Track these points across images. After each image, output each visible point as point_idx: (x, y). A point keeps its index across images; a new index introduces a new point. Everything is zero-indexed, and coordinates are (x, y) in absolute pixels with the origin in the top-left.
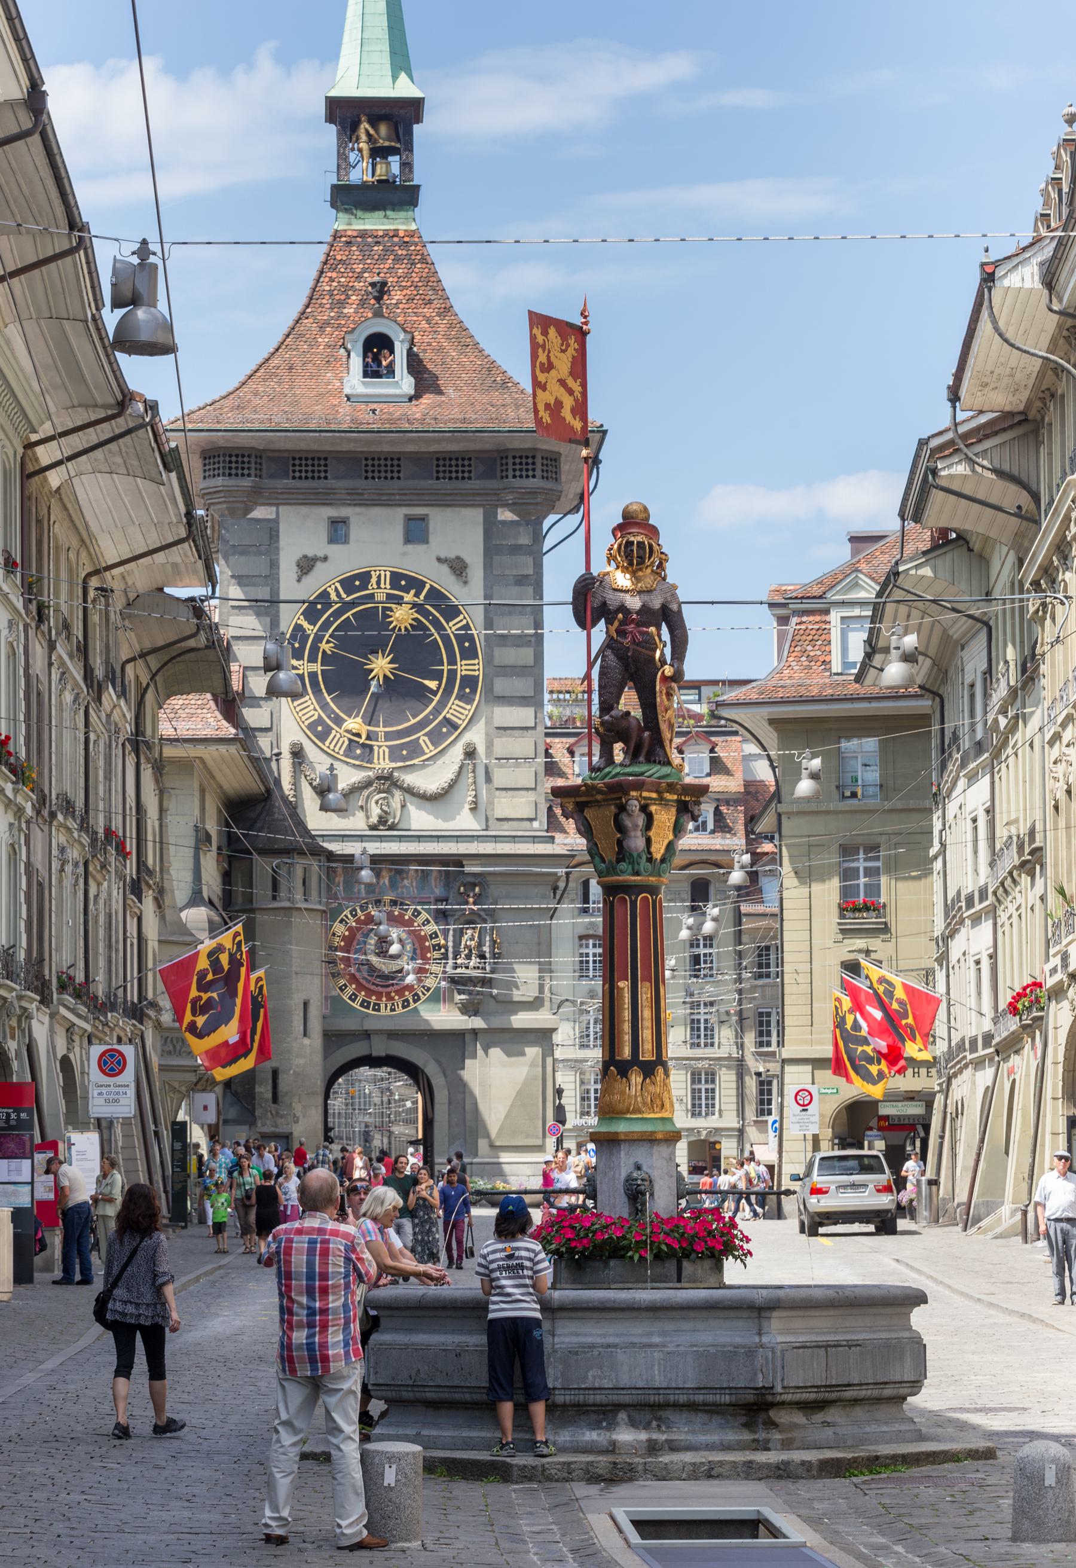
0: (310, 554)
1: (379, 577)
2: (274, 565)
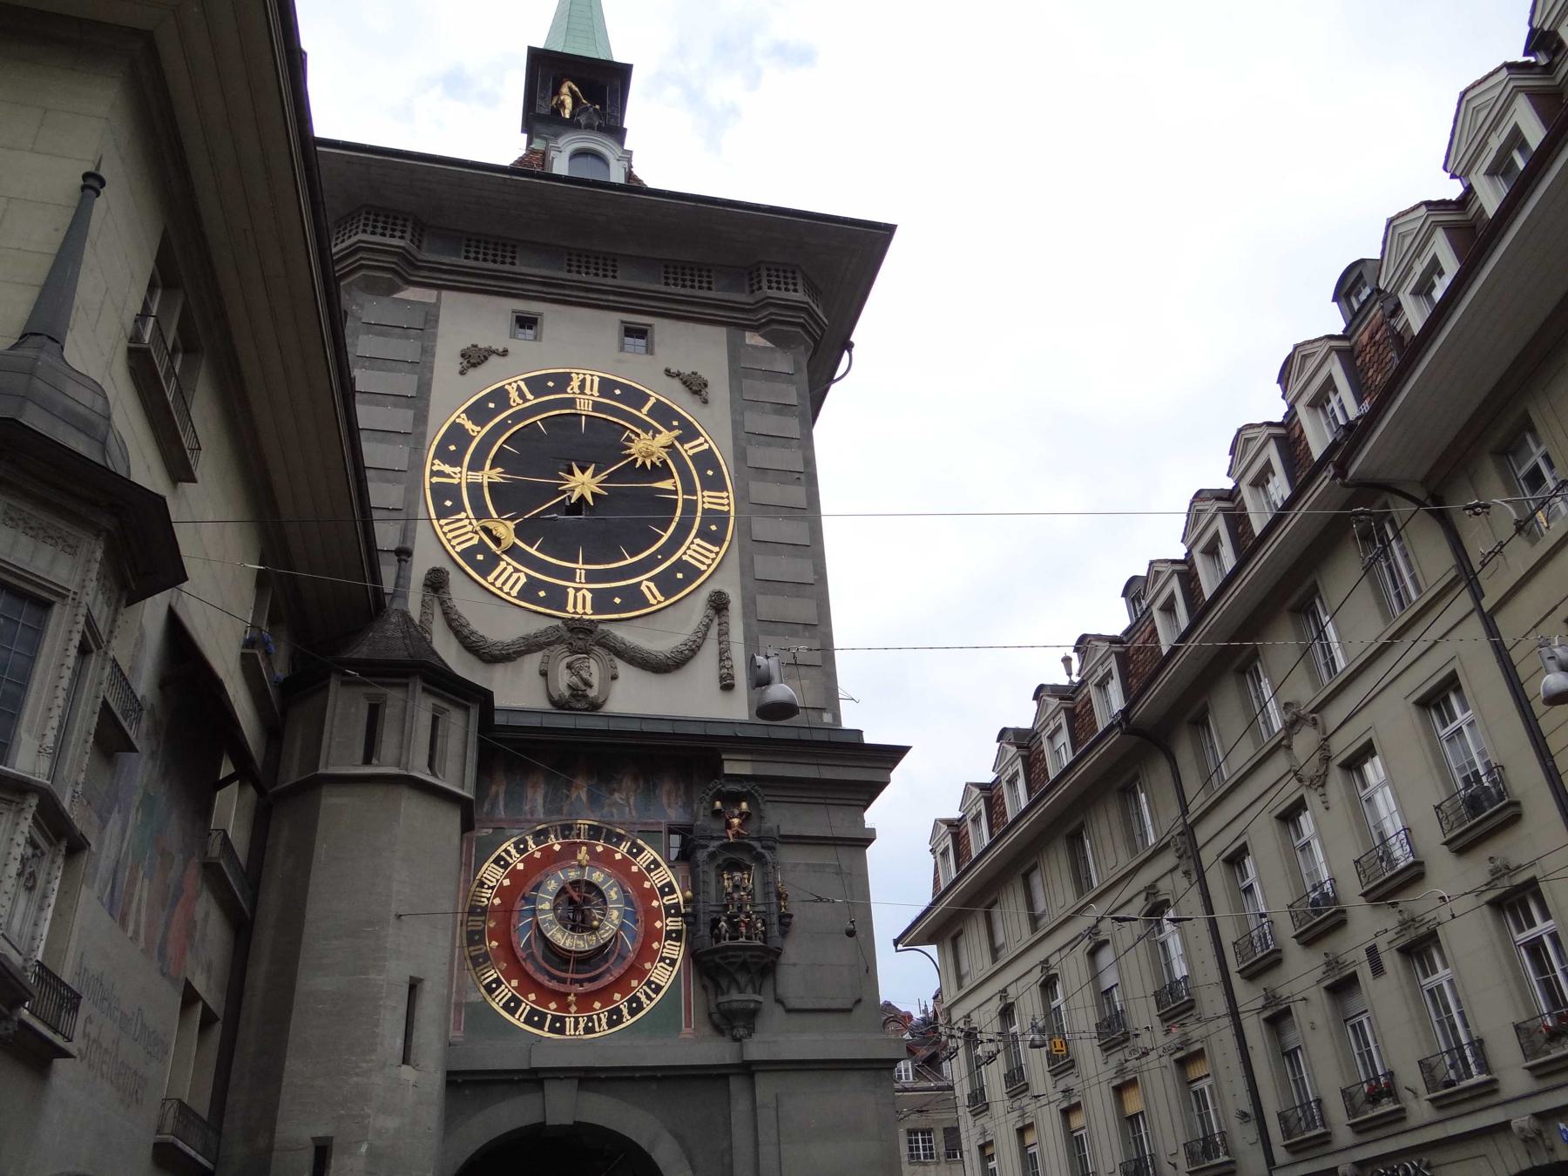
1: (583, 381)
2: (428, 352)
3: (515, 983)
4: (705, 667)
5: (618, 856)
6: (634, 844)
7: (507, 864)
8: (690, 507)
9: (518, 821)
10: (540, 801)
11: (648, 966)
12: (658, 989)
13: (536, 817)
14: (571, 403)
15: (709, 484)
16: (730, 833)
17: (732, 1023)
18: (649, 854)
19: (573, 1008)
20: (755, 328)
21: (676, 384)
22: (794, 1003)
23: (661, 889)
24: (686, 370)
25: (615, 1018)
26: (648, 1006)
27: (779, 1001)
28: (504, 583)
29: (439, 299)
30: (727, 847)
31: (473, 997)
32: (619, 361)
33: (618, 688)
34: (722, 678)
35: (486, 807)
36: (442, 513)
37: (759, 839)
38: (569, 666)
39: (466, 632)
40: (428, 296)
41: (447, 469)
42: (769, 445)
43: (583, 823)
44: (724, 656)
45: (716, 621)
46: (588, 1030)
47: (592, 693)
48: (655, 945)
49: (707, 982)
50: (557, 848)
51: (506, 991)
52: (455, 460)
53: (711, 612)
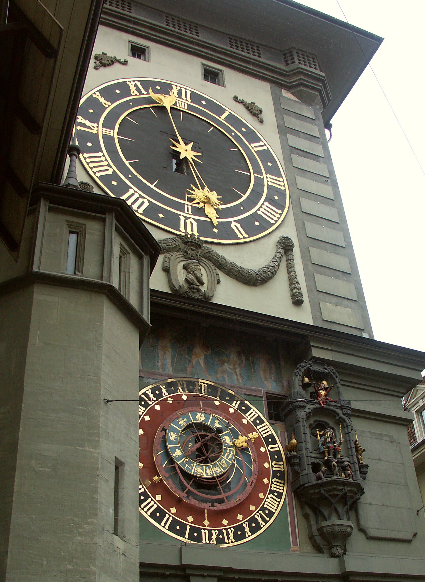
6: (242, 403)
9: (154, 374)
11: (261, 496)
12: (270, 514)
13: (166, 372)
17: (328, 542)
18: (254, 412)
19: (206, 522)
20: (289, 88)
21: (241, 107)
22: (373, 533)
27: (362, 530)
38: (185, 267)
42: (305, 157)
43: (203, 382)
44: (293, 282)
45: (284, 259)
46: (220, 541)
47: (203, 289)
49: (309, 511)
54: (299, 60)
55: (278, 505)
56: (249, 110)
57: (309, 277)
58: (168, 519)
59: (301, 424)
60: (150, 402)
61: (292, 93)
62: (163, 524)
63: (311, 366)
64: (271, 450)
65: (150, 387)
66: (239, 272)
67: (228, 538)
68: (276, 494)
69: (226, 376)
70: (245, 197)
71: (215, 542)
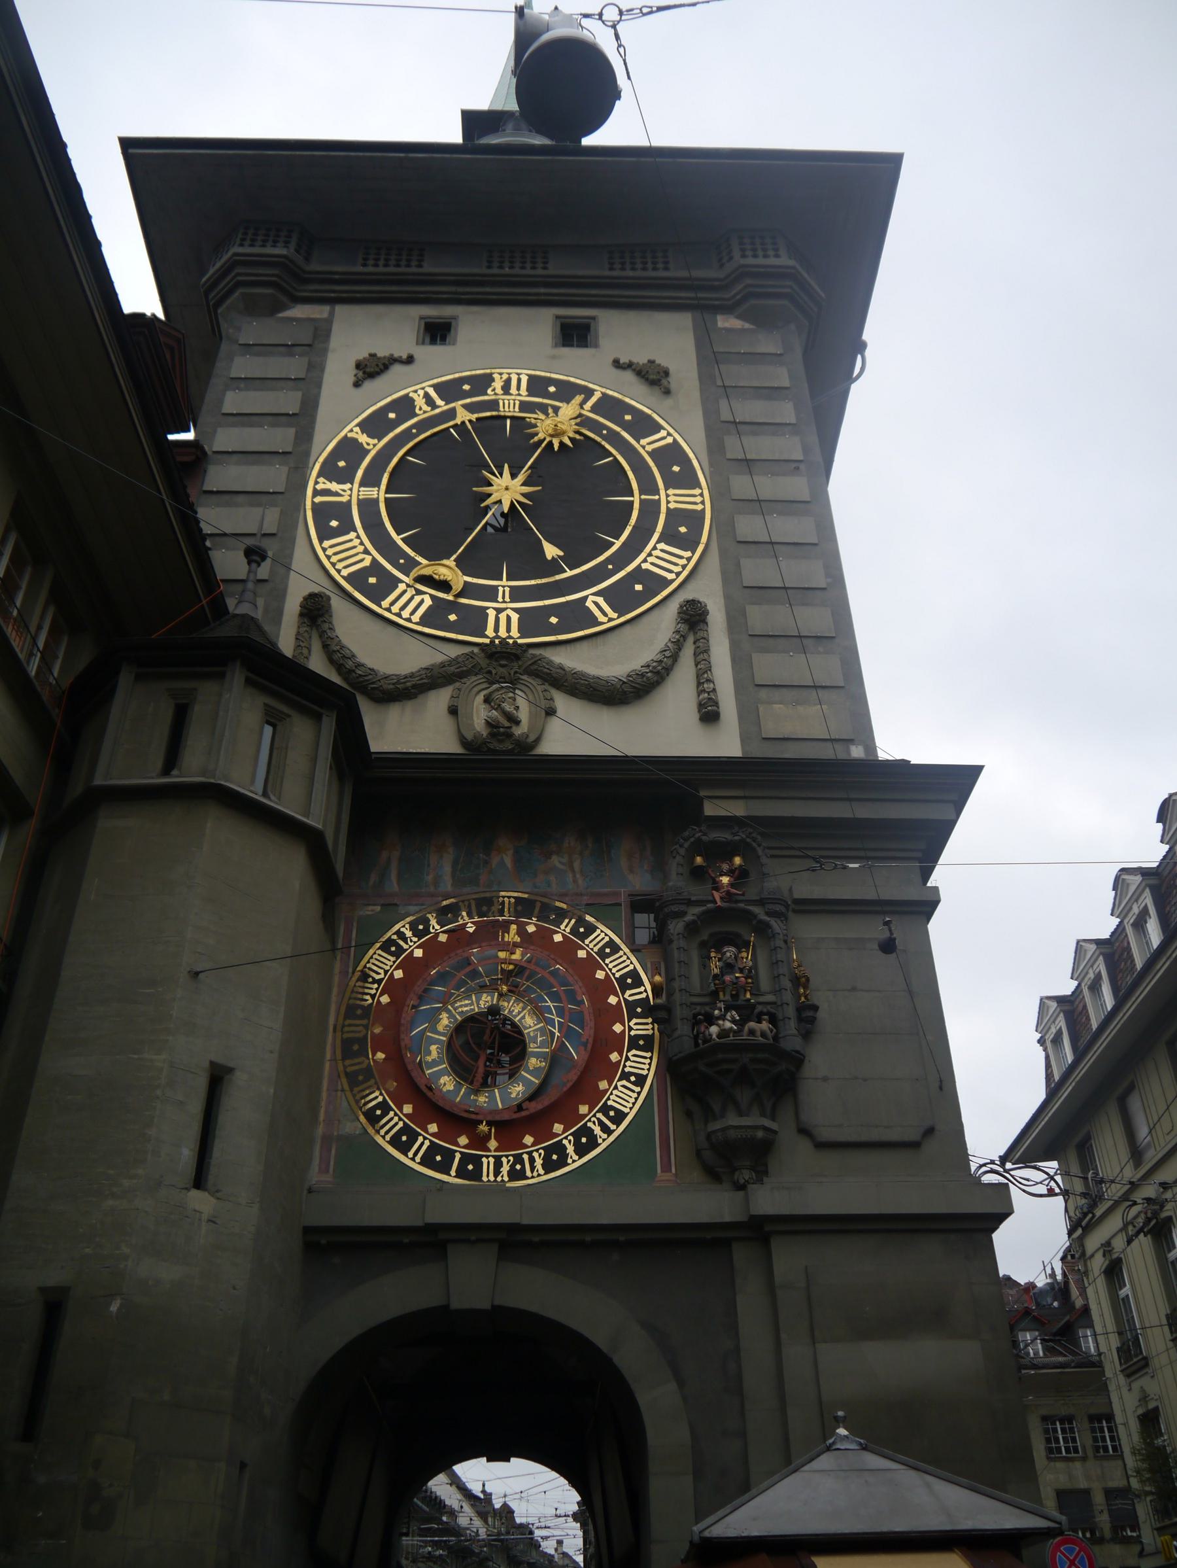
0: (381, 353)
3: (408, 1109)
4: (679, 693)
5: (558, 938)
6: (581, 921)
7: (401, 950)
8: (650, 510)
10: (447, 869)
11: (603, 1085)
12: (619, 1117)
14: (494, 405)
15: (672, 482)
16: (717, 895)
17: (733, 1160)
19: (493, 1144)
20: (728, 309)
21: (629, 376)
22: (826, 1134)
23: (621, 980)
24: (641, 359)
25: (555, 1158)
26: (605, 1142)
27: (804, 1131)
28: (403, 608)
29: (332, 313)
30: (716, 915)
31: (349, 1128)
32: (554, 357)
33: (555, 727)
34: (701, 705)
35: (373, 878)
36: (325, 533)
37: (761, 902)
39: (350, 664)
40: (318, 312)
41: (334, 486)
43: (508, 896)
46: (515, 1175)
48: (614, 1057)
50: (471, 929)
51: (395, 1121)
52: (345, 476)
53: (683, 627)
54: (743, 250)
55: (636, 1099)
56: (643, 377)
57: (740, 661)
58: (422, 1144)
59: (675, 945)
60: (405, 946)
61: (739, 317)
62: (410, 1154)
63: (705, 834)
64: (631, 999)
65: (408, 919)
66: (589, 686)
67: (533, 1168)
68: (633, 1079)
69: (552, 878)
70: (618, 544)
71: (506, 1178)
